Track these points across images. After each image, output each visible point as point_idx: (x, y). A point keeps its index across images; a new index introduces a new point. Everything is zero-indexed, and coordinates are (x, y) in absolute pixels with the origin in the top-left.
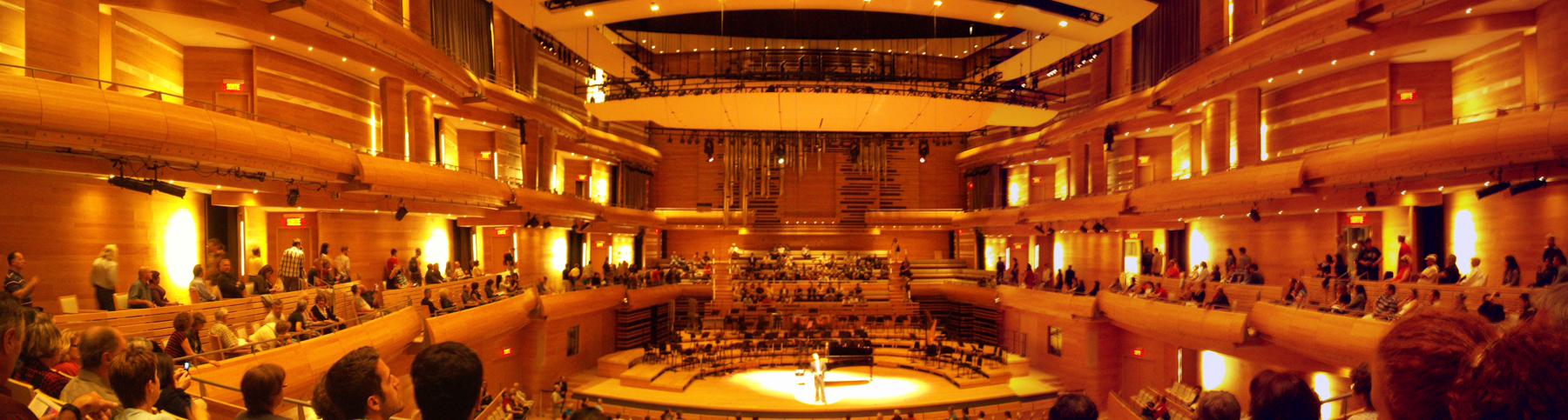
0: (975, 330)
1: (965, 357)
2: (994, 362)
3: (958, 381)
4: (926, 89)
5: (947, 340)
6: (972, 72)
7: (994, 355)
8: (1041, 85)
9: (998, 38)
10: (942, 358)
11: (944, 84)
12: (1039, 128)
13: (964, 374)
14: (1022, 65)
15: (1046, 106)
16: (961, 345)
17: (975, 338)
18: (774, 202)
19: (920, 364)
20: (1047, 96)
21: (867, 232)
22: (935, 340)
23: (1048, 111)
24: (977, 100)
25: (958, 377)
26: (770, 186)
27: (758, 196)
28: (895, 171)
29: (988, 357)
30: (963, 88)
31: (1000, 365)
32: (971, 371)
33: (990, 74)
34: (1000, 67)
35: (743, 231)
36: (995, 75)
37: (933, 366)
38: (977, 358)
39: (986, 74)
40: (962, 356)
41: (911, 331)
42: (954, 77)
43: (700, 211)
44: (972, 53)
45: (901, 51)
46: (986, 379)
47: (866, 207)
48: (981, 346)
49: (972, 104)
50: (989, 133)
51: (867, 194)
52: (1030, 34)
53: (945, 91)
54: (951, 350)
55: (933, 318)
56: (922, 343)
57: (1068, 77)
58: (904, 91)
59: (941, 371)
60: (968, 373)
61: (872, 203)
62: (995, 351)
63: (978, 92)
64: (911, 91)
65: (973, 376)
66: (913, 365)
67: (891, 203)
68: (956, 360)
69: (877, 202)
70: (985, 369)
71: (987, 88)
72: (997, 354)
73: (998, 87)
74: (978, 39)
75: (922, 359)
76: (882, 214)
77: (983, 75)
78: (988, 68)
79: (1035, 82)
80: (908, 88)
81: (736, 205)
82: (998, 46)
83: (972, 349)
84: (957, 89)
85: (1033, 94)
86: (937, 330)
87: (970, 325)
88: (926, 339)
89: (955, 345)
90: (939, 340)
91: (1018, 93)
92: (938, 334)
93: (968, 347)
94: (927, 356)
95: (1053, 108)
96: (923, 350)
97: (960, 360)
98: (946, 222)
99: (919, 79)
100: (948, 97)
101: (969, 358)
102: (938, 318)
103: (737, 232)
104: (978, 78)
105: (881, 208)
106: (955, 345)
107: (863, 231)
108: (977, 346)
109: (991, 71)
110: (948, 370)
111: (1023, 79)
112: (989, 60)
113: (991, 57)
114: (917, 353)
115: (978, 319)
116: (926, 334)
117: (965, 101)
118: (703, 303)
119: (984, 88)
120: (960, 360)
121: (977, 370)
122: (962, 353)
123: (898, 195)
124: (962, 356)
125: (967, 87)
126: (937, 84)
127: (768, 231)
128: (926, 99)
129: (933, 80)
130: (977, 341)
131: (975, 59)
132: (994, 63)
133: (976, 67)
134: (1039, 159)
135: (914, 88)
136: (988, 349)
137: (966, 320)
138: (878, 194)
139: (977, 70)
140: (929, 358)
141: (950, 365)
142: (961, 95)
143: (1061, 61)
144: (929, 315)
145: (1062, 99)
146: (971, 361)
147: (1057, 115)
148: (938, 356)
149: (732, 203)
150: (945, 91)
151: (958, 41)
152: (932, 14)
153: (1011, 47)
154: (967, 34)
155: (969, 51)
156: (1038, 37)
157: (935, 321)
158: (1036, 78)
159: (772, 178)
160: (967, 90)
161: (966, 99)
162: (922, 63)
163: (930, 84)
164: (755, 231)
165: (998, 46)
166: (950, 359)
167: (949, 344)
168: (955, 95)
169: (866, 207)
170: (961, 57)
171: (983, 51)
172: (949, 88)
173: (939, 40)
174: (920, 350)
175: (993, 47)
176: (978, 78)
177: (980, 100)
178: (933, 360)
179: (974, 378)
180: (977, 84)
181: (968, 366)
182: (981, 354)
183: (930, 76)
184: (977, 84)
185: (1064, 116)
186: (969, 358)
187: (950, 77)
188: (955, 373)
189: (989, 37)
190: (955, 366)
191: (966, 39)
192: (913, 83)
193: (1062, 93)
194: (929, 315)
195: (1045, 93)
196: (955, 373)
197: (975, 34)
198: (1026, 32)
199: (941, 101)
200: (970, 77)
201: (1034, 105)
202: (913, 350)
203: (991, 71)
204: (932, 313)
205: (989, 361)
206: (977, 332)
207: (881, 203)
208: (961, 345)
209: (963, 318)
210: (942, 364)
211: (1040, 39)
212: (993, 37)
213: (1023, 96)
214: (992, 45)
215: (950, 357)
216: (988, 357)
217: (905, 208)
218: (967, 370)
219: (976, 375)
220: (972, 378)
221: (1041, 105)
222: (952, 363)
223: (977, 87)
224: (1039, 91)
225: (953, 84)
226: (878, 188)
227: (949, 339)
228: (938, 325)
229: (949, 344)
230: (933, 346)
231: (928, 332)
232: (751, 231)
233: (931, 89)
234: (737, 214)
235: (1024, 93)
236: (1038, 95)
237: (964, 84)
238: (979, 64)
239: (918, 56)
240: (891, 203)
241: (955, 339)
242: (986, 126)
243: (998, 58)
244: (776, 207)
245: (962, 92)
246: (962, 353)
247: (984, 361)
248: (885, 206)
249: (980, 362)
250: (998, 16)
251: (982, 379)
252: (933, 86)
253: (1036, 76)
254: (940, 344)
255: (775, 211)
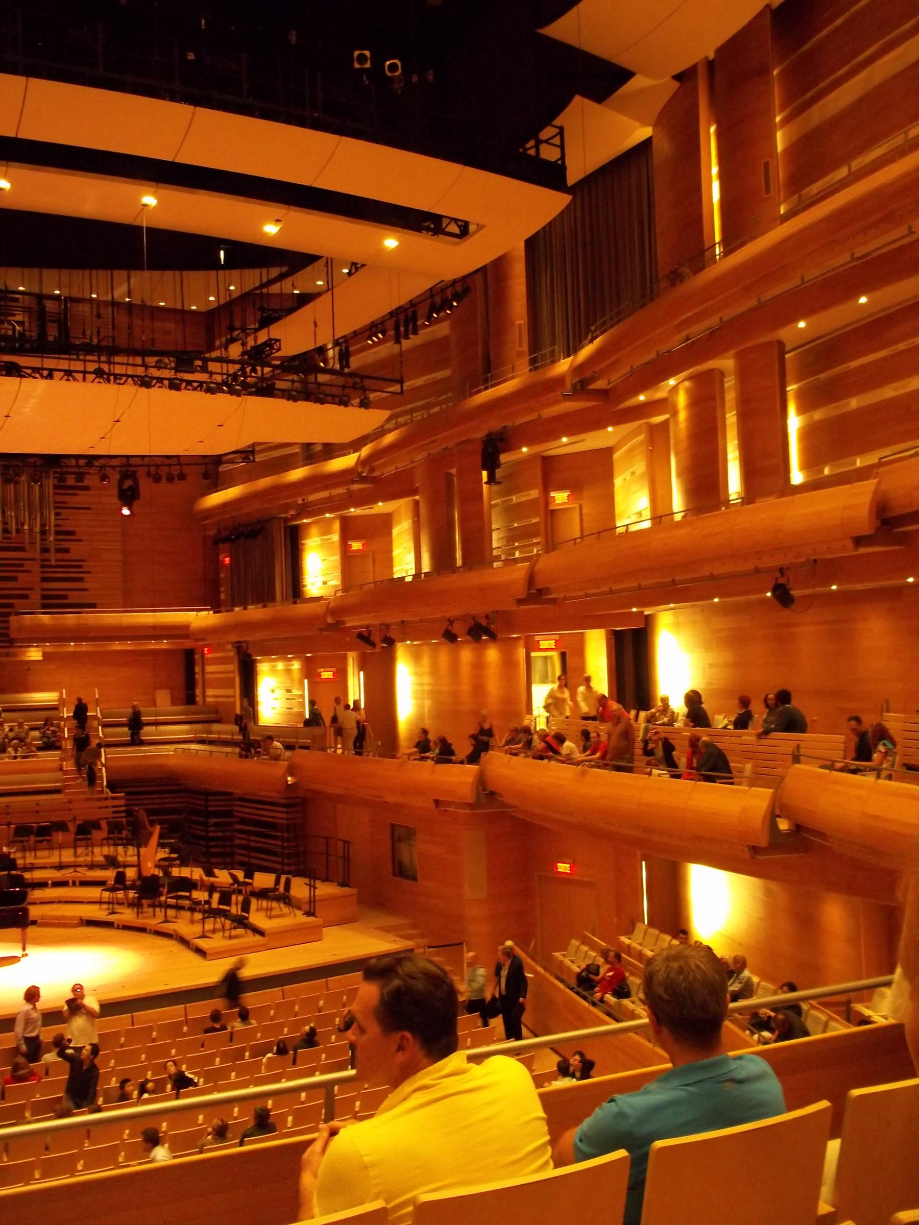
0: (237, 842)
1: (216, 896)
2: (275, 904)
3: (203, 944)
4: (130, 371)
5: (180, 866)
6: (224, 339)
7: (275, 889)
8: (355, 362)
9: (275, 272)
10: (171, 901)
11: (166, 360)
12: (355, 445)
13: (214, 931)
14: (316, 326)
15: (364, 404)
16: (210, 873)
17: (238, 858)
19: (127, 915)
20: (367, 383)
21: (15, 655)
22: (157, 866)
23: (371, 411)
24: (232, 392)
25: (203, 936)
28: (72, 533)
29: (263, 894)
30: (204, 369)
31: (286, 910)
32: (228, 923)
33: (259, 342)
34: (275, 331)
36: (270, 343)
37: (154, 917)
38: (240, 898)
39: (251, 342)
40: (210, 896)
41: (106, 850)
42: (189, 348)
44: (222, 302)
45: (75, 293)
46: (258, 938)
47: (11, 606)
48: (249, 875)
49: (223, 400)
50: (258, 458)
51: (15, 579)
52: (330, 263)
53: (167, 374)
54: (188, 884)
55: (152, 823)
56: (131, 873)
57: (406, 344)
58: (85, 373)
59: (170, 927)
60: (223, 929)
61: (26, 597)
62: (277, 882)
63: (235, 376)
64: (99, 373)
65: (234, 932)
66: (112, 918)
67: (65, 597)
68: (199, 903)
69: (35, 597)
70: (257, 918)
71: (255, 371)
72: (281, 888)
73: (275, 367)
74: (236, 273)
75: (131, 905)
76: (45, 619)
77: (243, 344)
78: (256, 330)
79: (344, 357)
80: (91, 367)
82: (275, 289)
83: (231, 881)
84: (193, 372)
85: (340, 381)
86: (161, 845)
87: (228, 834)
88: (138, 866)
89: (197, 873)
90: (165, 869)
91: (311, 378)
92: (163, 854)
93: (223, 877)
94: (140, 898)
95: (380, 405)
96: (133, 887)
97: (208, 902)
98: (180, 632)
99: (113, 351)
100: (174, 386)
101: (225, 899)
102: (161, 822)
104: (235, 351)
105: (44, 606)
106: (197, 873)
107: (8, 655)
108: (240, 875)
109: (262, 337)
110: (184, 925)
111: (322, 350)
112: (259, 314)
113: (262, 309)
114: (120, 895)
115: (243, 821)
116: (138, 855)
117: (209, 395)
119: (248, 370)
120: (208, 902)
121: (241, 922)
122: (211, 889)
123: (80, 580)
124: (210, 896)
125: (213, 366)
126: (151, 360)
128: (129, 390)
129: (143, 353)
130: (242, 865)
131: (231, 313)
132: (265, 323)
133: (231, 329)
134: (357, 505)
135: (105, 367)
136: (263, 880)
137: (216, 824)
138: (39, 579)
139: (235, 334)
140: (145, 902)
141: (187, 914)
142: (201, 383)
143: (392, 314)
144: (142, 815)
145: (396, 388)
146: (229, 903)
147: (389, 420)
148: (163, 898)
150: (167, 374)
151: (195, 278)
152: (137, 223)
153: (296, 292)
154: (215, 265)
155: (218, 298)
156: (346, 271)
157: (157, 829)
158: (347, 348)
160: (211, 373)
161: (209, 390)
162: (122, 319)
163: (139, 360)
165: (275, 289)
166: (186, 903)
167: (185, 872)
168: (189, 383)
169: (11, 606)
170: (203, 309)
171: (245, 298)
172: (177, 370)
173: (157, 274)
174: (126, 888)
175: (264, 291)
176: (235, 351)
177: (238, 394)
178: (153, 906)
179: (236, 937)
180: (233, 362)
181: (225, 914)
182: (249, 889)
183: (137, 345)
184: (233, 362)
185: (401, 420)
186: (225, 899)
187: (180, 348)
188: (198, 929)
189: (257, 271)
190: (198, 916)
191: (213, 273)
192: (103, 359)
193: (397, 376)
194: (142, 815)
195: (362, 377)
196: (198, 929)
197: (231, 264)
198: (323, 261)
199: (160, 394)
200: (220, 348)
201: (345, 403)
202: (113, 889)
203: (262, 337)
204: (150, 812)
205: (265, 903)
206: (241, 847)
207: (44, 597)
208: (210, 873)
209: (212, 821)
210: (171, 913)
211: (350, 274)
212: (264, 271)
213: (319, 385)
214: (262, 286)
215: (189, 898)
216: (263, 894)
217: (93, 606)
218: (220, 921)
219: (241, 931)
220: (231, 937)
221: (356, 401)
222: (192, 910)
223: (233, 368)
224: (352, 375)
225: (184, 361)
226: (36, 568)
227: (184, 863)
228: (161, 836)
229: (185, 872)
230: (154, 877)
231: (142, 850)
233: (140, 371)
235: (322, 378)
236: (350, 381)
237: (205, 361)
238: (237, 324)
239: (114, 304)
240: (65, 597)
241: (197, 863)
242: (254, 445)
243: (275, 311)
245: (203, 377)
246: (211, 889)
247: (254, 903)
248: (52, 603)
249: (246, 907)
250: (271, 229)
251: (253, 939)
252: (145, 366)
253: (345, 346)
254: (167, 874)
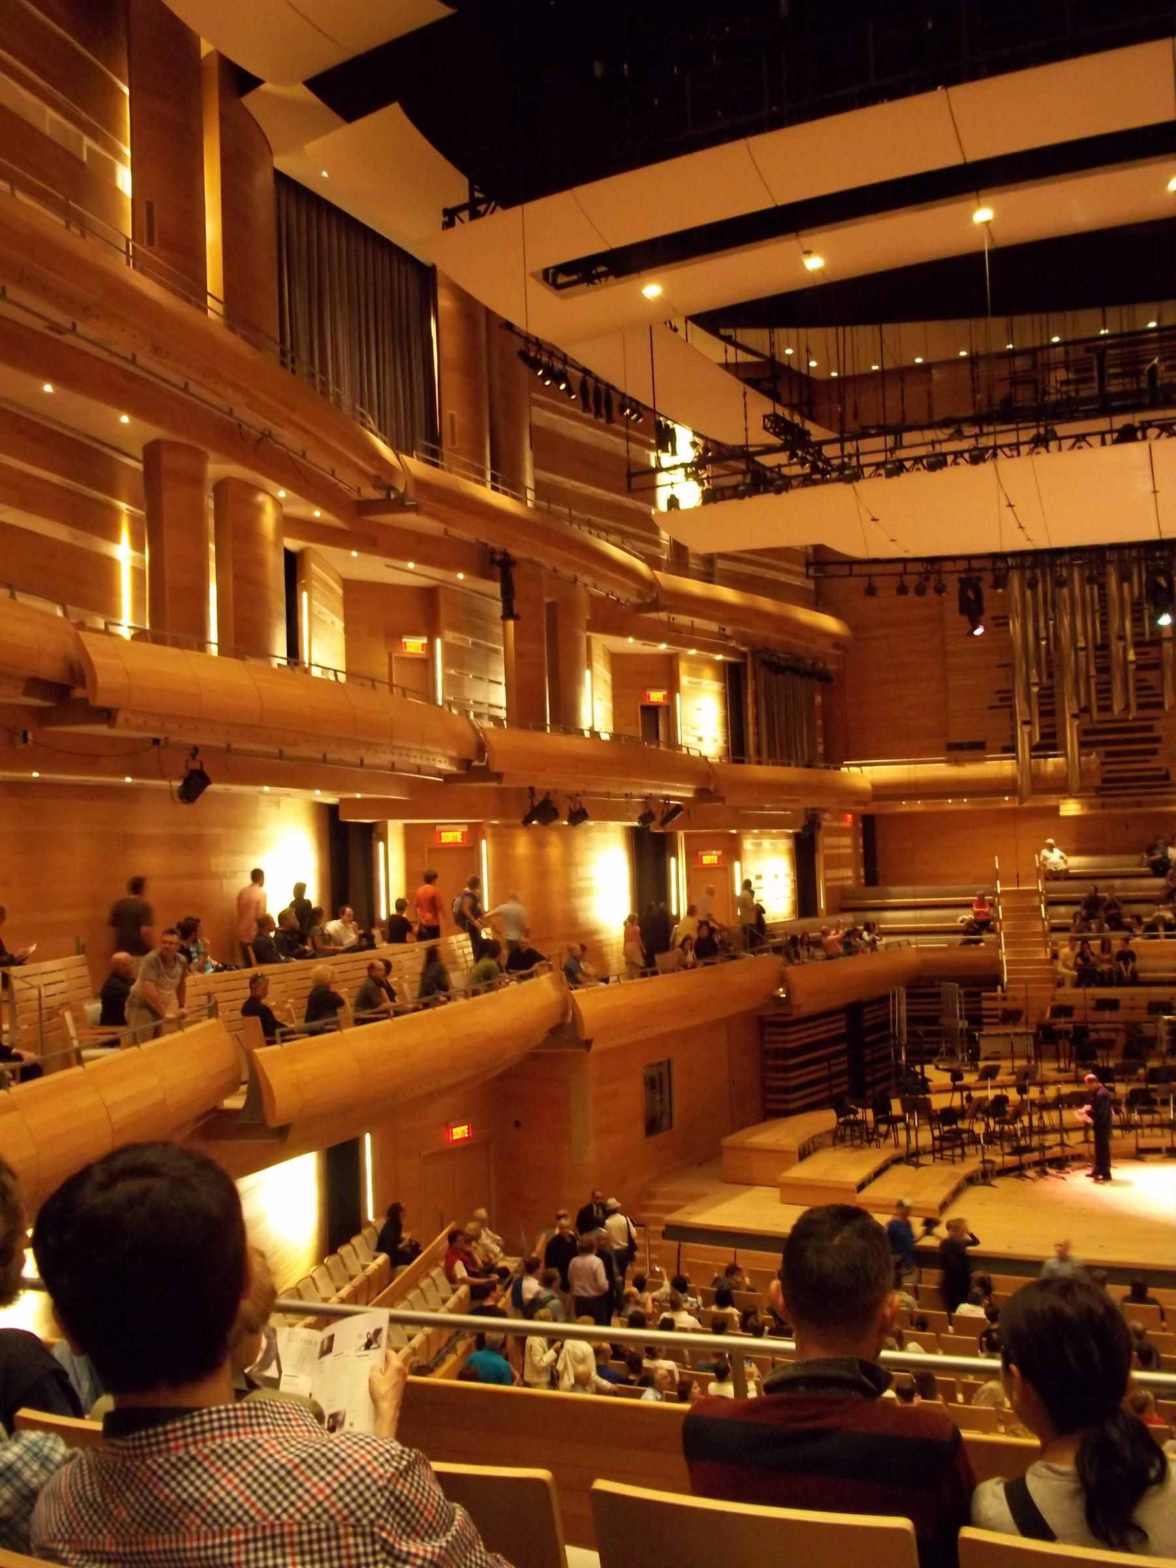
18: (1150, 729)
26: (1138, 689)
27: (1107, 716)
35: (1070, 808)
43: (957, 762)
81: (1048, 744)
103: (1057, 808)
118: (978, 994)
127: (1139, 804)
149: (1037, 738)
159: (1140, 667)
164: (1103, 806)
232: (1091, 807)
234: (1051, 764)
244: (1157, 740)
255: (1154, 752)
